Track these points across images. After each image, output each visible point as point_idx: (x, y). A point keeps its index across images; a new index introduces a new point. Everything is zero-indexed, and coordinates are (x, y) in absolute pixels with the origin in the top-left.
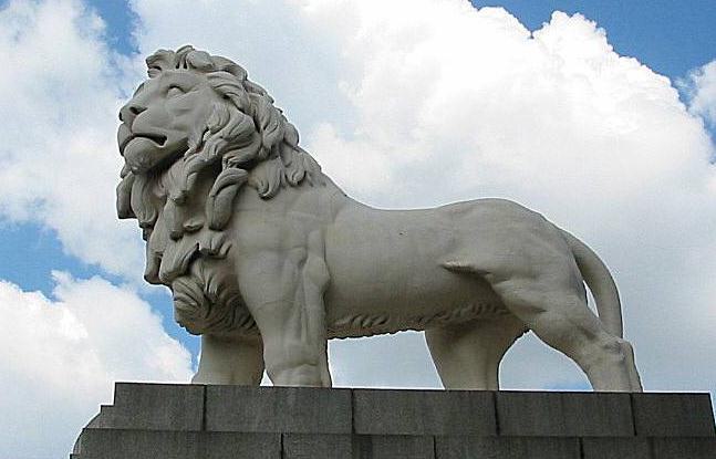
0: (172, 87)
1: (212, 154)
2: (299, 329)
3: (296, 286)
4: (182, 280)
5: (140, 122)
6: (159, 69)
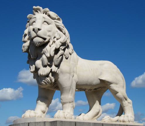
0: (45, 22)
1: (59, 47)
2: (71, 93)
3: (72, 82)
4: (47, 78)
5: (40, 33)
6: (37, 12)
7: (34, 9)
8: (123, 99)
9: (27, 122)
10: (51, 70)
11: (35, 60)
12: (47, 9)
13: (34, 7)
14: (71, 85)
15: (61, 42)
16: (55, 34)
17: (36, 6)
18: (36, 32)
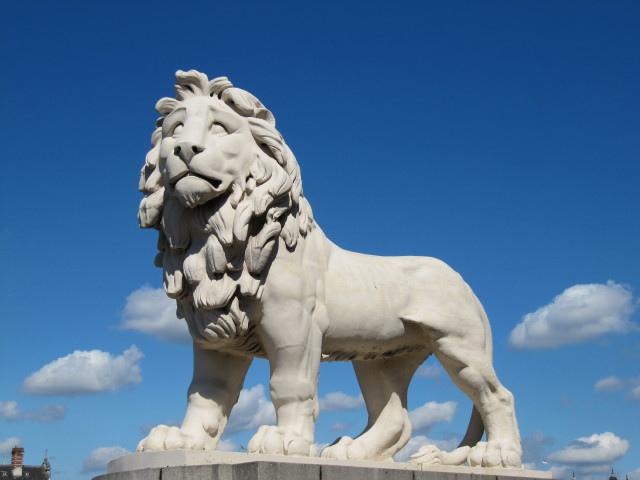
0: (216, 123)
1: (263, 209)
2: (307, 368)
3: (309, 330)
4: (223, 316)
7: (180, 81)
8: (482, 388)
9: (155, 467)
10: (238, 287)
11: (183, 253)
12: (224, 81)
13: (180, 73)
14: (307, 339)
15: (270, 193)
16: (251, 164)
17: (186, 70)
18: (187, 158)
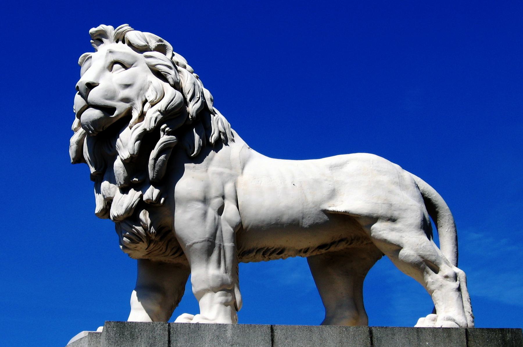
3: (216, 228)
5: (94, 95)
7: (91, 37)
12: (125, 27)
13: (92, 30)
14: (214, 235)
15: (160, 111)
16: (147, 91)
17: (96, 27)
18: (84, 94)
